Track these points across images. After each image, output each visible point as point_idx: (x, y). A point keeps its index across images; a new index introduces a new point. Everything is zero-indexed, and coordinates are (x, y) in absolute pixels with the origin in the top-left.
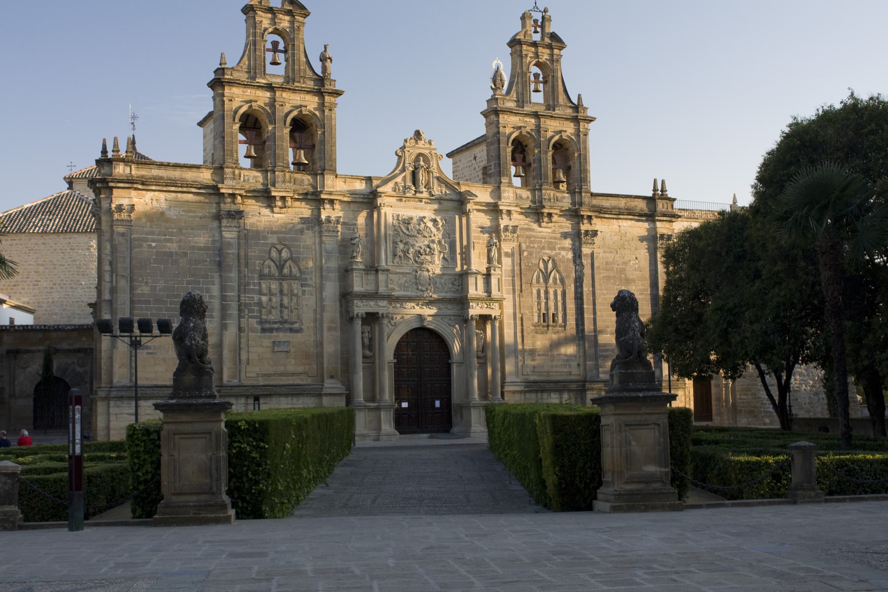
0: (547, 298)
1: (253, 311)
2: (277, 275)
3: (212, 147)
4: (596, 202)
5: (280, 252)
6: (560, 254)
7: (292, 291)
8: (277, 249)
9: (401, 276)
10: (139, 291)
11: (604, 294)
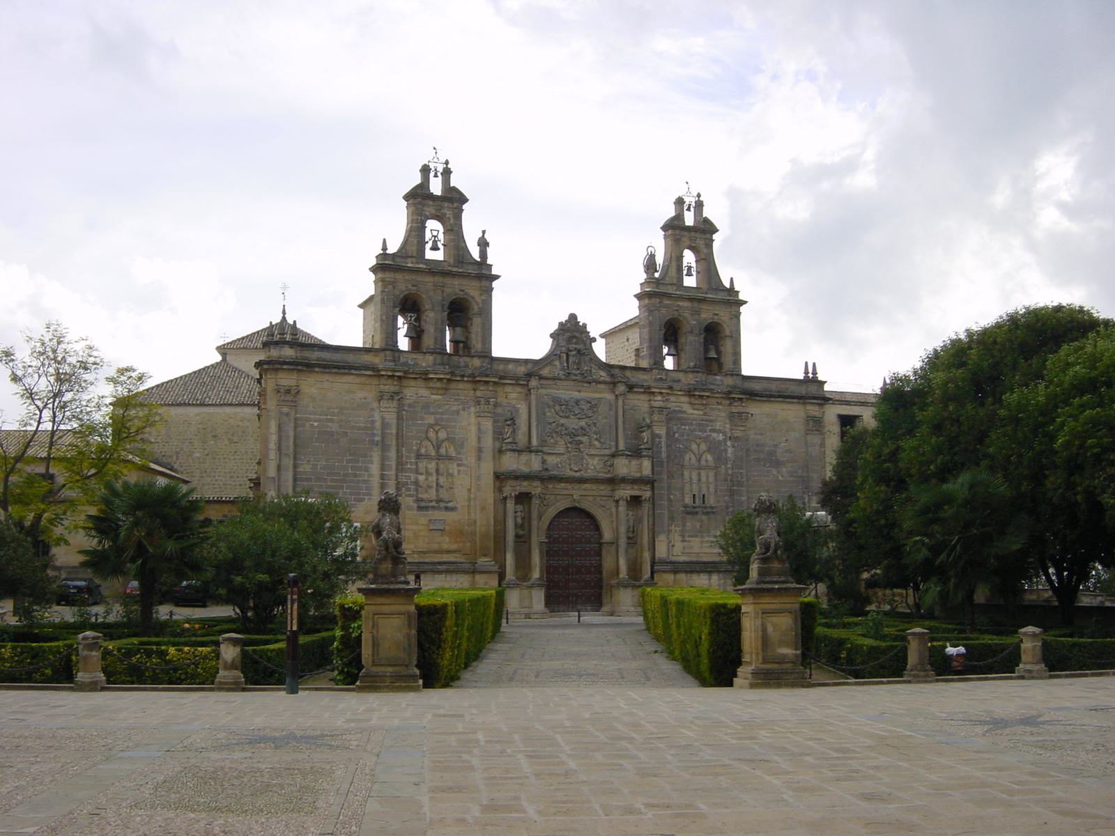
0: (699, 480)
1: (408, 490)
2: (433, 454)
3: (373, 330)
4: (749, 385)
5: (437, 433)
7: (448, 470)
8: (434, 429)
10: (301, 469)
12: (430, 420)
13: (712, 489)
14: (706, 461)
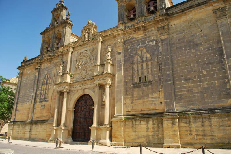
0: (142, 69)
6: (148, 44)
9: (77, 75)
11: (178, 57)
12: (46, 73)
13: (150, 72)
14: (147, 58)
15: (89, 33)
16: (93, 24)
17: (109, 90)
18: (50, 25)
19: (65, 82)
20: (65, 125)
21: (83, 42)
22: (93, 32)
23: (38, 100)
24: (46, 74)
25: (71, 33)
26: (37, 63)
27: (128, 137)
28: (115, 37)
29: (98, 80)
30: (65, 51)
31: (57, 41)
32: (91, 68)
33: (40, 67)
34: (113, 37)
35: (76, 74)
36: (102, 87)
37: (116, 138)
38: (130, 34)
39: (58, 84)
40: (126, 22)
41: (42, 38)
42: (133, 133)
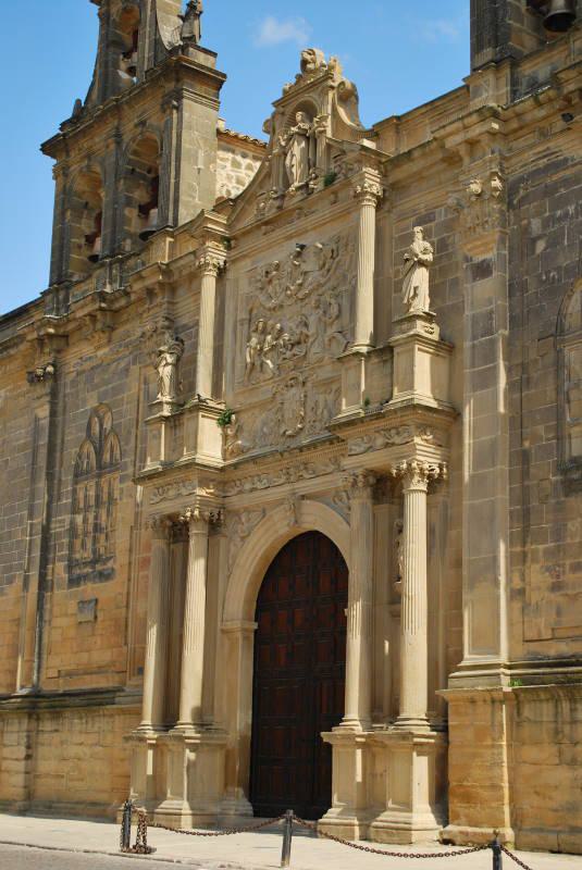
9: (256, 411)
12: (92, 403)
15: (311, 139)
16: (328, 76)
17: (429, 506)
18: (93, 84)
19: (191, 465)
20: (207, 718)
21: (277, 203)
22: (329, 134)
23: (59, 570)
24: (95, 411)
25: (219, 132)
26: (41, 341)
27: (537, 793)
28: (452, 159)
29: (362, 449)
30: (182, 262)
31: (140, 195)
32: (326, 372)
33: (53, 365)
34: (443, 160)
35: (253, 407)
36: (386, 489)
37: (468, 798)
38: (545, 135)
39: (151, 476)
40: (529, 42)
41: (55, 178)
42: (563, 775)
